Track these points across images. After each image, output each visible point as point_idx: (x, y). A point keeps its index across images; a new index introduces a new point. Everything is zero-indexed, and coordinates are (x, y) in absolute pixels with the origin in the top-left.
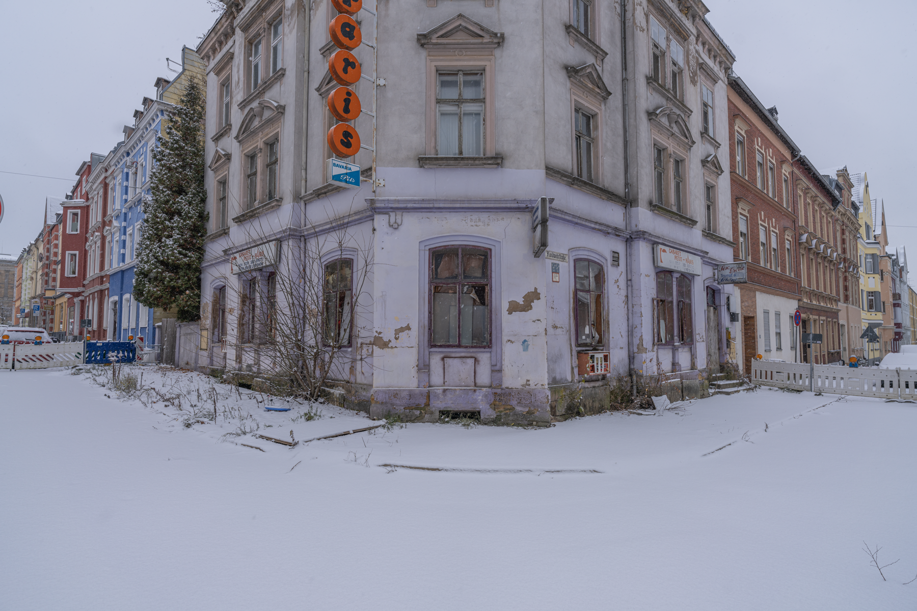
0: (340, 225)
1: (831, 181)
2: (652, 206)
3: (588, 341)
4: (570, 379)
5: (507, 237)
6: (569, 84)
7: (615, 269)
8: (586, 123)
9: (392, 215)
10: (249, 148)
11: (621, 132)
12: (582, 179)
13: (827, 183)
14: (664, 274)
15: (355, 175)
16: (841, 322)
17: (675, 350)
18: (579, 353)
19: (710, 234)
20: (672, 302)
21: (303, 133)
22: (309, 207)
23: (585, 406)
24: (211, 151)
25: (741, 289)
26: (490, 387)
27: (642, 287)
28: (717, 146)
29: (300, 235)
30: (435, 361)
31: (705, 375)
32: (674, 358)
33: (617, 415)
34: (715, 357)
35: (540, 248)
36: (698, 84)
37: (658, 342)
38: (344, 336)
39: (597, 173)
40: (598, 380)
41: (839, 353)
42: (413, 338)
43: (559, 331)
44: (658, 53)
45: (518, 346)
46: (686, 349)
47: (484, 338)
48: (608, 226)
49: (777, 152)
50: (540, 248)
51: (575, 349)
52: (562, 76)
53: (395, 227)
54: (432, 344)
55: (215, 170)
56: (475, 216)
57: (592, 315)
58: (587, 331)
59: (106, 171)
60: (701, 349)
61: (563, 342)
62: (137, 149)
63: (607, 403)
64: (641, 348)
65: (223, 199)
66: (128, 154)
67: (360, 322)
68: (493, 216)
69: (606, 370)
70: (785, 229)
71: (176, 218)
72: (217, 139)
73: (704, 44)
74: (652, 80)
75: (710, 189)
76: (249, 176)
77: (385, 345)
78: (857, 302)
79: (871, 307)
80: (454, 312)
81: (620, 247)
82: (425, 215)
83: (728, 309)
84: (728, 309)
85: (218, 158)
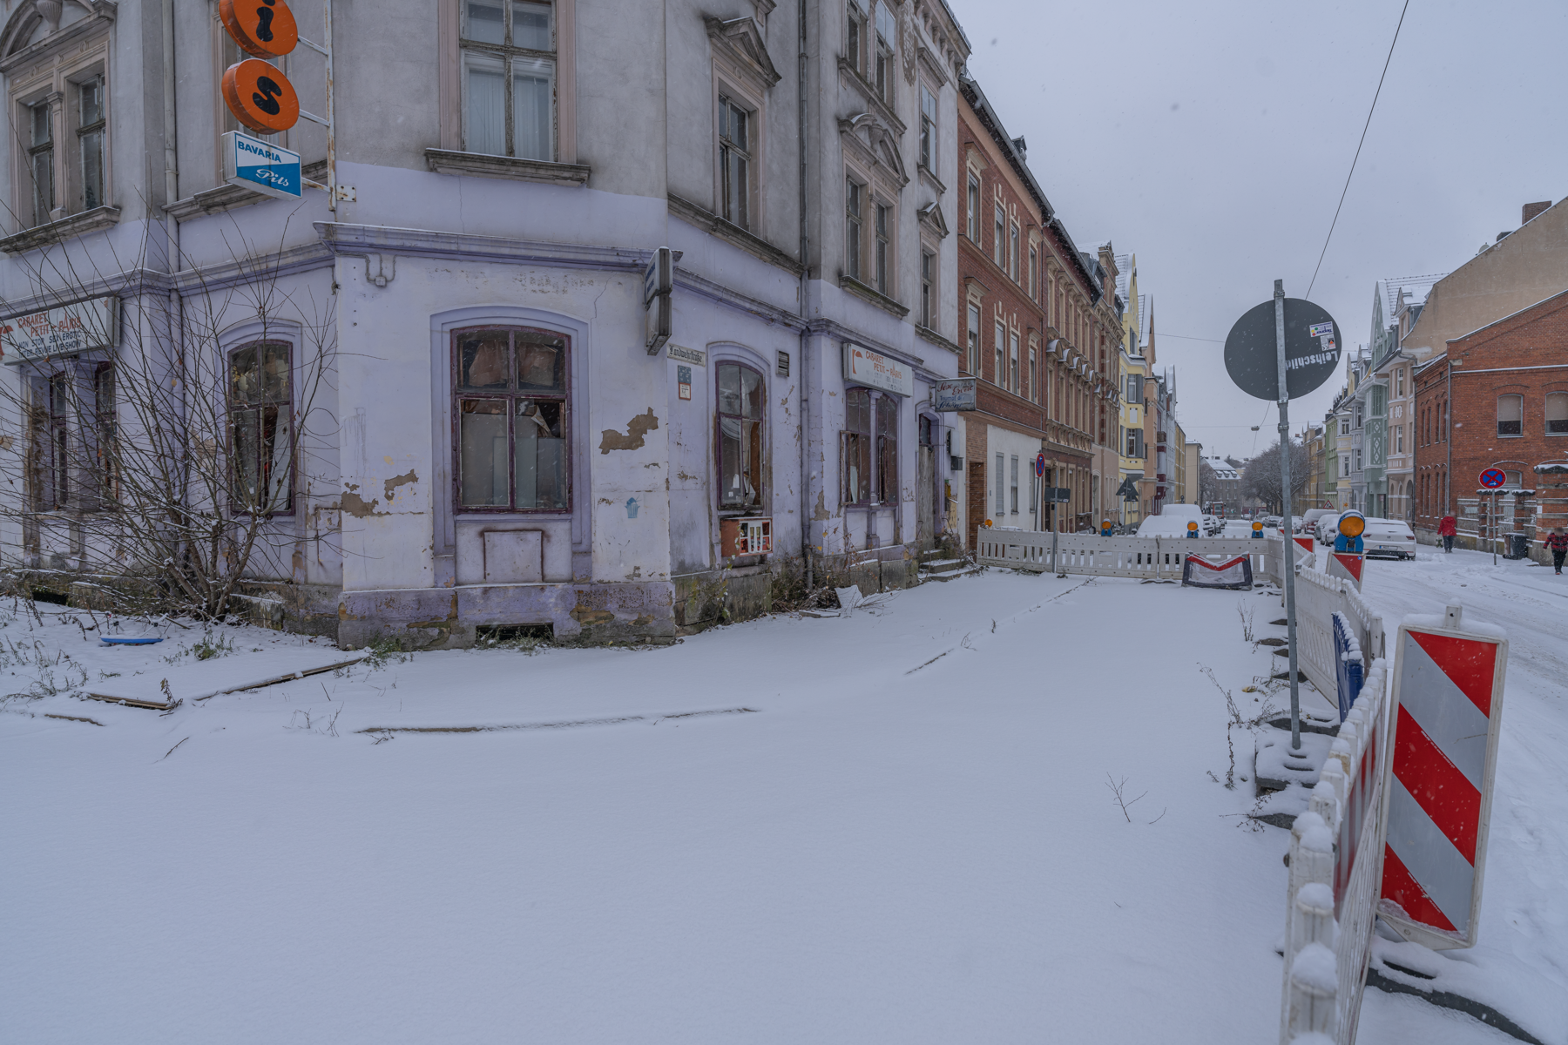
0: (260, 271)
1: (1091, 262)
2: (843, 280)
3: (738, 500)
4: (707, 564)
5: (598, 316)
7: (782, 380)
8: (738, 122)
11: (795, 147)
12: (729, 223)
13: (1086, 265)
14: (856, 392)
15: (289, 171)
16: (1095, 472)
17: (871, 513)
18: (723, 519)
19: (927, 332)
20: (868, 438)
21: (163, 72)
22: (186, 230)
23: (731, 608)
25: (967, 420)
26: (571, 581)
27: (825, 414)
28: (941, 190)
29: (167, 289)
30: (468, 539)
31: (913, 552)
32: (869, 526)
33: (783, 619)
34: (928, 525)
35: (658, 338)
37: (846, 502)
38: (278, 495)
39: (755, 216)
40: (753, 565)
41: (1089, 517)
42: (423, 496)
43: (690, 483)
44: (856, 18)
45: (620, 509)
46: (888, 513)
47: (558, 495)
48: (772, 308)
49: (1023, 210)
50: (658, 338)
51: (716, 514)
52: (697, 31)
53: (381, 283)
54: (459, 510)
56: (540, 273)
57: (745, 457)
58: (736, 484)
60: (909, 511)
61: (696, 503)
63: (766, 600)
64: (821, 513)
67: (312, 466)
69: (766, 548)
70: (1030, 329)
73: (926, 16)
74: (846, 63)
75: (928, 258)
76: (33, 151)
77: (365, 510)
78: (1115, 445)
79: (1131, 451)
80: (501, 447)
81: (791, 345)
82: (441, 264)
83: (949, 450)
84: (949, 450)
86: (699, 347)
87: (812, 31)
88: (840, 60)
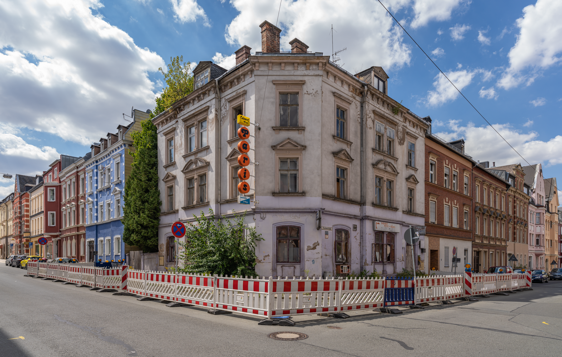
2: (374, 205)
5: (307, 223)
6: (334, 159)
8: (341, 173)
9: (262, 214)
10: (190, 176)
11: (359, 174)
14: (379, 234)
24: (162, 173)
30: (279, 268)
36: (405, 143)
42: (271, 259)
43: (328, 257)
47: (297, 259)
52: (331, 157)
53: (263, 219)
54: (277, 262)
55: (166, 182)
56: (294, 214)
57: (343, 251)
59: (77, 168)
62: (104, 160)
65: (171, 196)
66: (97, 162)
68: (301, 214)
71: (146, 204)
72: (166, 167)
73: (410, 122)
80: (286, 249)
82: (275, 214)
85: (168, 176)
86: (330, 226)
87: (364, 144)
88: (374, 150)
